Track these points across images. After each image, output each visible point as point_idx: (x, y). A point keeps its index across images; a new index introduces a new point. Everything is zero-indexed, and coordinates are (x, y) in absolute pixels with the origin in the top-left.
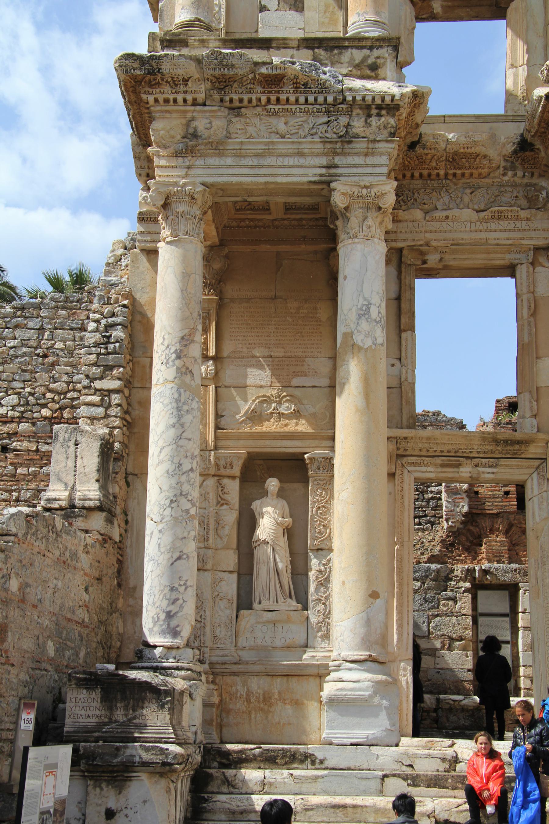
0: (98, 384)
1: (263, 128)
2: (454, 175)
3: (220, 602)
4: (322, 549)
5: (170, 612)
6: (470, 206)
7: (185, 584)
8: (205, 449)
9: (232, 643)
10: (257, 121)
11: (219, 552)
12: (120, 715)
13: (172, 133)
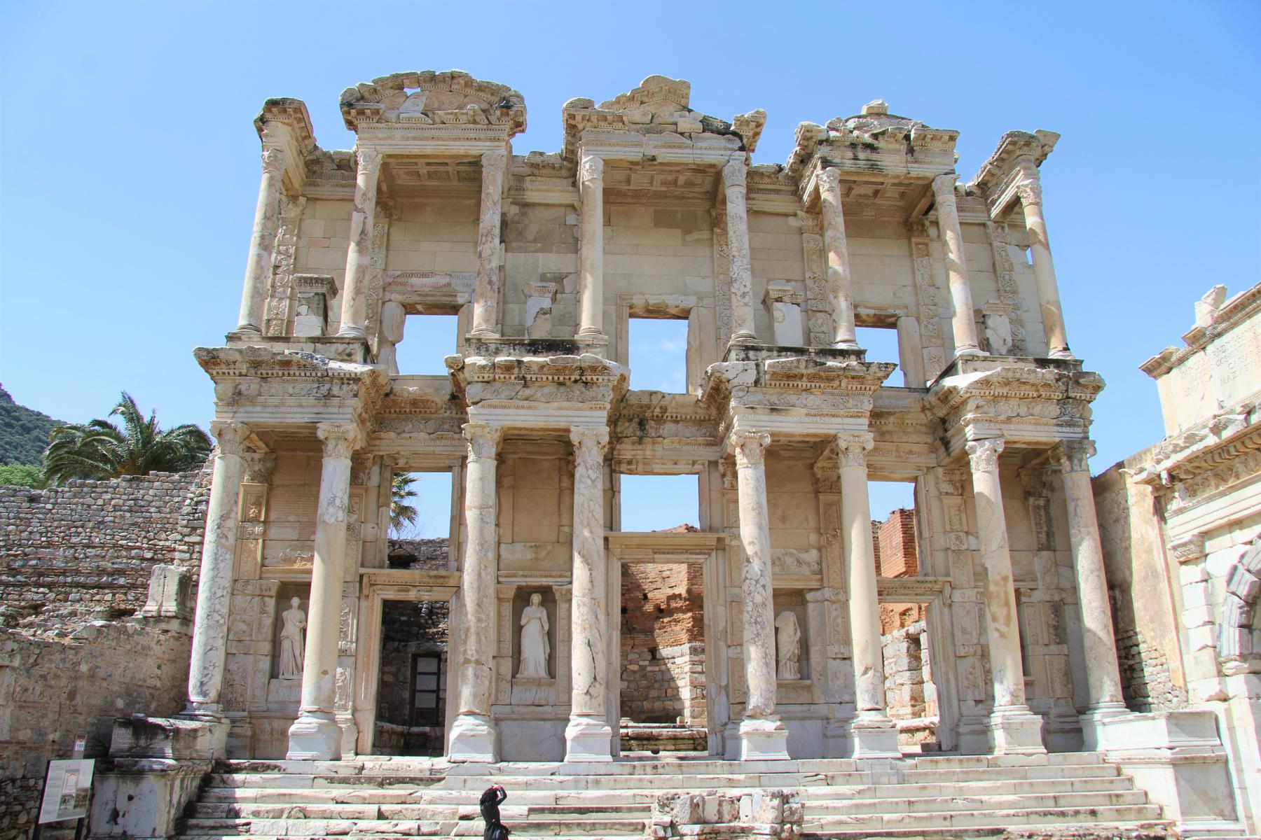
0: (187, 539)
12: (142, 742)
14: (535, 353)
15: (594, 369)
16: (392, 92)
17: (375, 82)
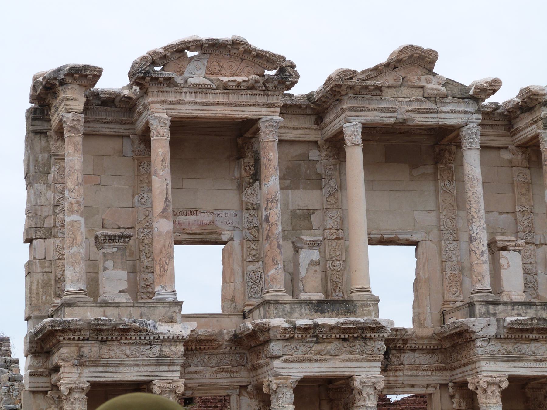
1: (118, 351)
2: (200, 348)
10: (115, 348)
13: (72, 355)
14: (322, 312)
15: (372, 329)
16: (177, 55)
17: (165, 49)
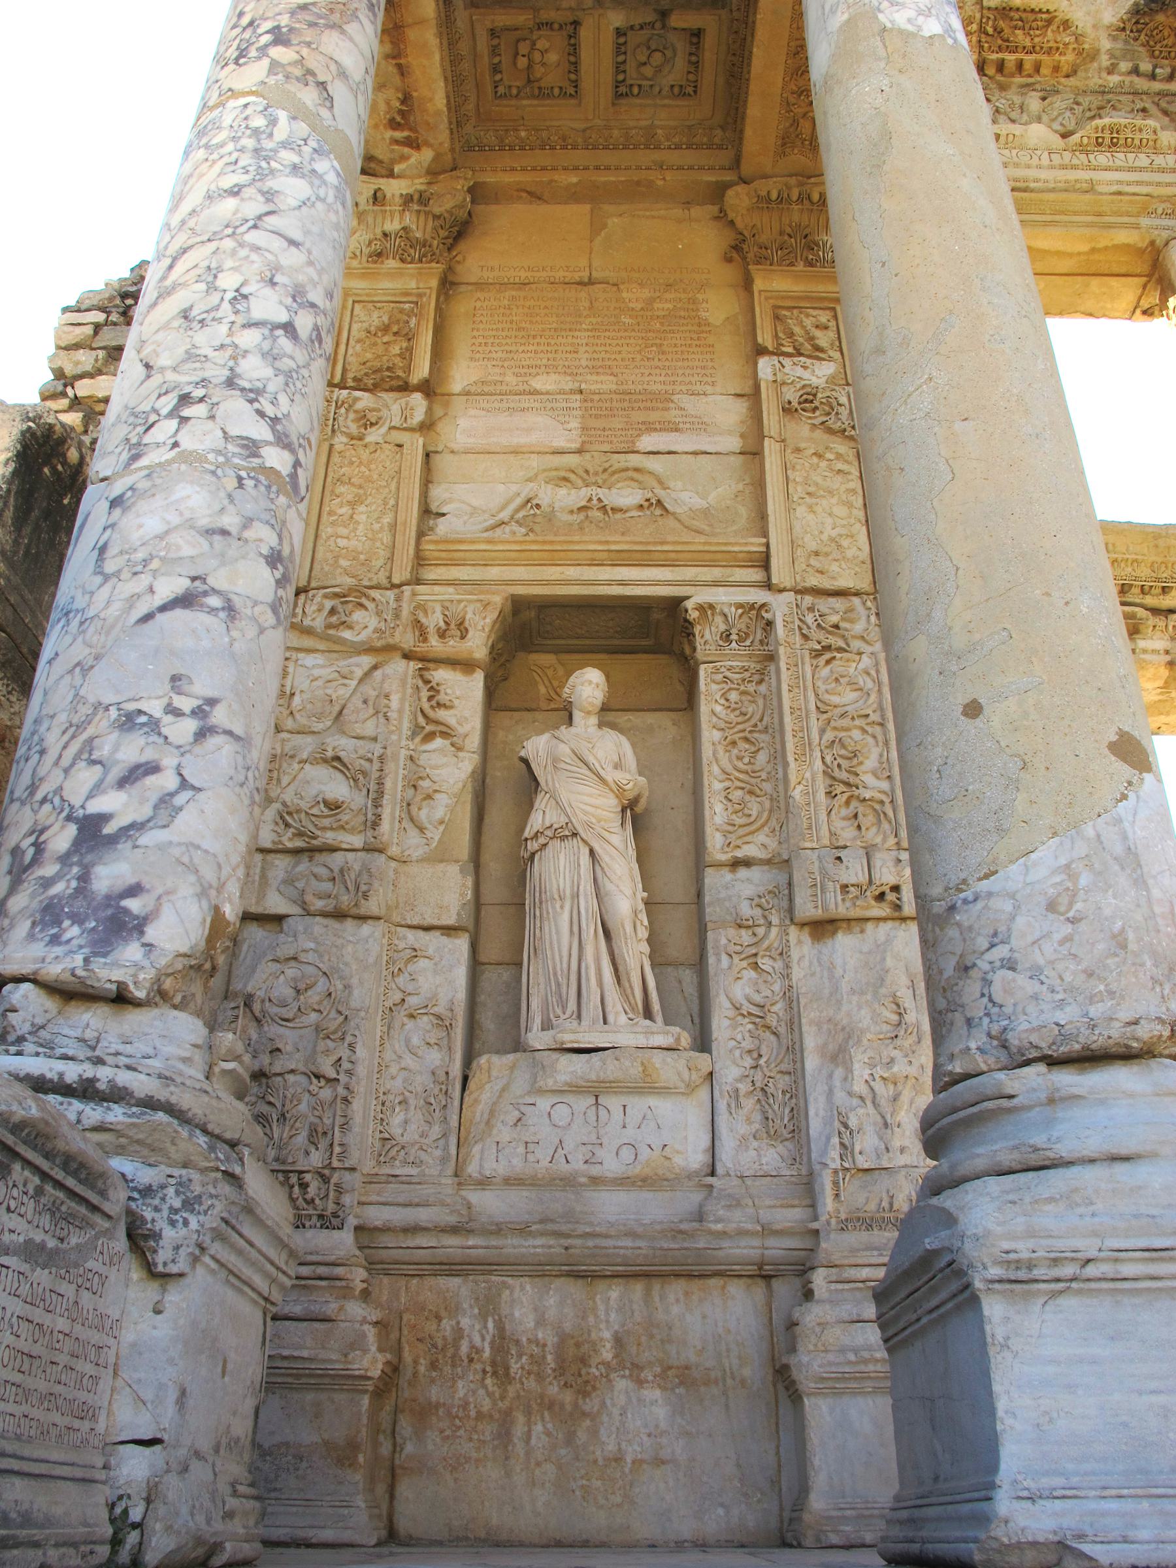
3: (410, 1024)
4: (747, 863)
5: (104, 818)
6: (1045, 118)
7: (197, 712)
8: (385, 582)
9: (444, 1160)
11: (414, 869)
